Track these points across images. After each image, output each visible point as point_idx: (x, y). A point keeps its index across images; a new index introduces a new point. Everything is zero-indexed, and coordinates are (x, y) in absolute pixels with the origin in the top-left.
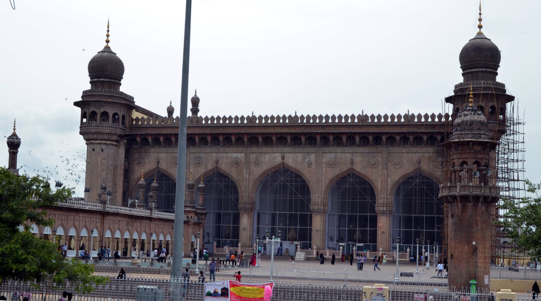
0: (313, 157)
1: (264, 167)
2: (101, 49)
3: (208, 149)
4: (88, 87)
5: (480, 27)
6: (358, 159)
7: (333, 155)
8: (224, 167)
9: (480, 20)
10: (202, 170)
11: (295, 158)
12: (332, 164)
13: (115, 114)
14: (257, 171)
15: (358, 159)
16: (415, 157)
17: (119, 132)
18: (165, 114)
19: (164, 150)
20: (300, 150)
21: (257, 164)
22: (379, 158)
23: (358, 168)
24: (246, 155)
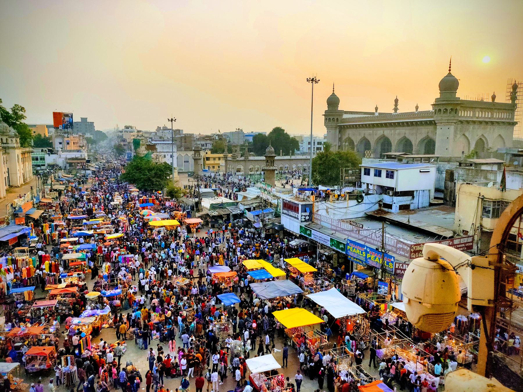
0: (393, 131)
3: (361, 129)
5: (450, 70)
6: (407, 132)
8: (366, 136)
9: (450, 67)
11: (387, 132)
12: (399, 134)
14: (376, 137)
15: (407, 132)
16: (427, 130)
17: (335, 125)
19: (350, 130)
20: (389, 128)
22: (414, 131)
24: (373, 132)
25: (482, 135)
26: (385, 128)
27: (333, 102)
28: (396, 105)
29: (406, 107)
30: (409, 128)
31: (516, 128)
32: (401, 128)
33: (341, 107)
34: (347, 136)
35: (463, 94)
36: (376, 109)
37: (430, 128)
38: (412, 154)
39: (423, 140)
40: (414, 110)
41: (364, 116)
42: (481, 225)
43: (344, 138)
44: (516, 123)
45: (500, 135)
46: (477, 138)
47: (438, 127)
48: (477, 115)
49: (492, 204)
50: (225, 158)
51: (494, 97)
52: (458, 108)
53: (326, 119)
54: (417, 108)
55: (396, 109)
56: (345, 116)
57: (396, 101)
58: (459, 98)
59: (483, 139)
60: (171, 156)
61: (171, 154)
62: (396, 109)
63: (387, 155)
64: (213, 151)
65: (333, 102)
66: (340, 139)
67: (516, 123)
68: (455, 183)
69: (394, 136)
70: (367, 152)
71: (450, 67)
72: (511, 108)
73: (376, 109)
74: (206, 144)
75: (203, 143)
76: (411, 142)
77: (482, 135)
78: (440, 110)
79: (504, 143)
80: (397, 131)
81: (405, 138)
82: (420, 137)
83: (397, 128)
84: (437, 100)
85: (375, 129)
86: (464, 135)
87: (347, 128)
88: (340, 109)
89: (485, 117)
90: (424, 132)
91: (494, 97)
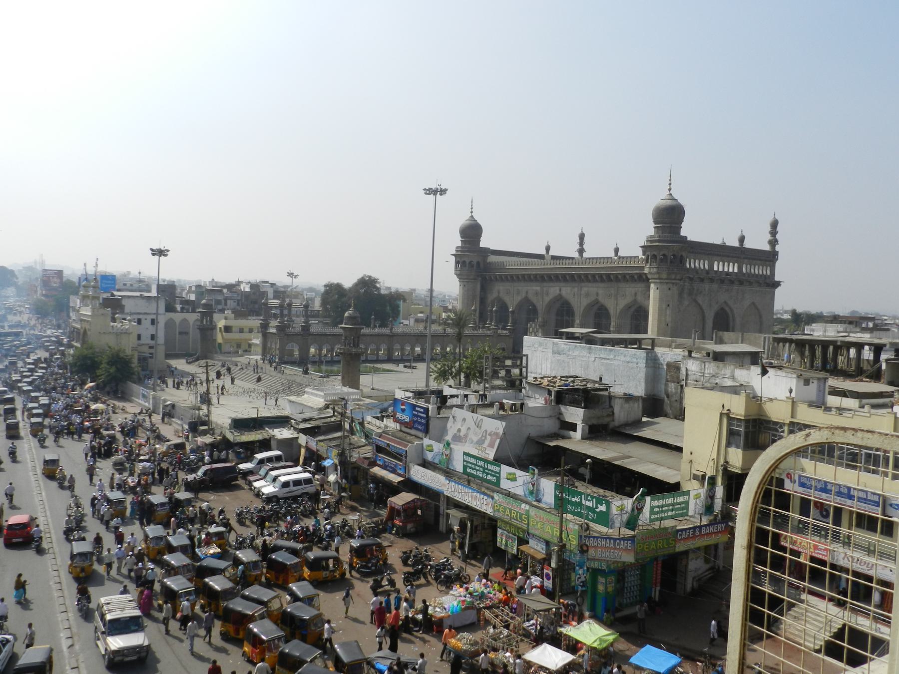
0: (576, 289)
1: (551, 297)
2: (468, 216)
4: (460, 245)
5: (670, 189)
7: (586, 289)
9: (670, 184)
10: (520, 298)
11: (567, 291)
12: (587, 295)
13: (470, 262)
14: (547, 299)
15: (601, 292)
18: (544, 252)
21: (547, 294)
23: (601, 299)
25: (725, 302)
26: (562, 284)
27: (471, 232)
28: (581, 243)
29: (599, 249)
30: (602, 285)
31: (778, 291)
32: (590, 285)
33: (486, 242)
34: (495, 295)
35: (691, 230)
36: (548, 249)
37: (640, 286)
38: (610, 332)
39: (628, 307)
40: (612, 254)
41: (525, 259)
42: (726, 462)
43: (492, 296)
44: (778, 284)
45: (753, 303)
46: (716, 308)
47: (652, 285)
48: (716, 268)
49: (743, 424)
50: (264, 326)
51: (742, 240)
52: (684, 254)
53: (457, 262)
54: (617, 251)
55: (581, 251)
56: (492, 259)
57: (582, 237)
58: (686, 237)
59: (727, 309)
60: (153, 322)
61: (154, 317)
62: (581, 251)
63: (567, 333)
64: (238, 314)
65: (471, 232)
66: (483, 301)
67: (778, 284)
68: (682, 386)
69: (579, 297)
70: (531, 326)
71: (670, 184)
72: (769, 257)
73: (548, 249)
74: (226, 300)
75: (220, 298)
76: (606, 309)
77: (725, 302)
78: (654, 257)
79: (761, 317)
80: (585, 290)
81: (597, 302)
82: (623, 303)
83: (583, 284)
84: (650, 240)
85: (545, 284)
86: (695, 301)
87: (497, 280)
88: (482, 245)
89: (728, 274)
90: (630, 291)
91: (742, 240)
